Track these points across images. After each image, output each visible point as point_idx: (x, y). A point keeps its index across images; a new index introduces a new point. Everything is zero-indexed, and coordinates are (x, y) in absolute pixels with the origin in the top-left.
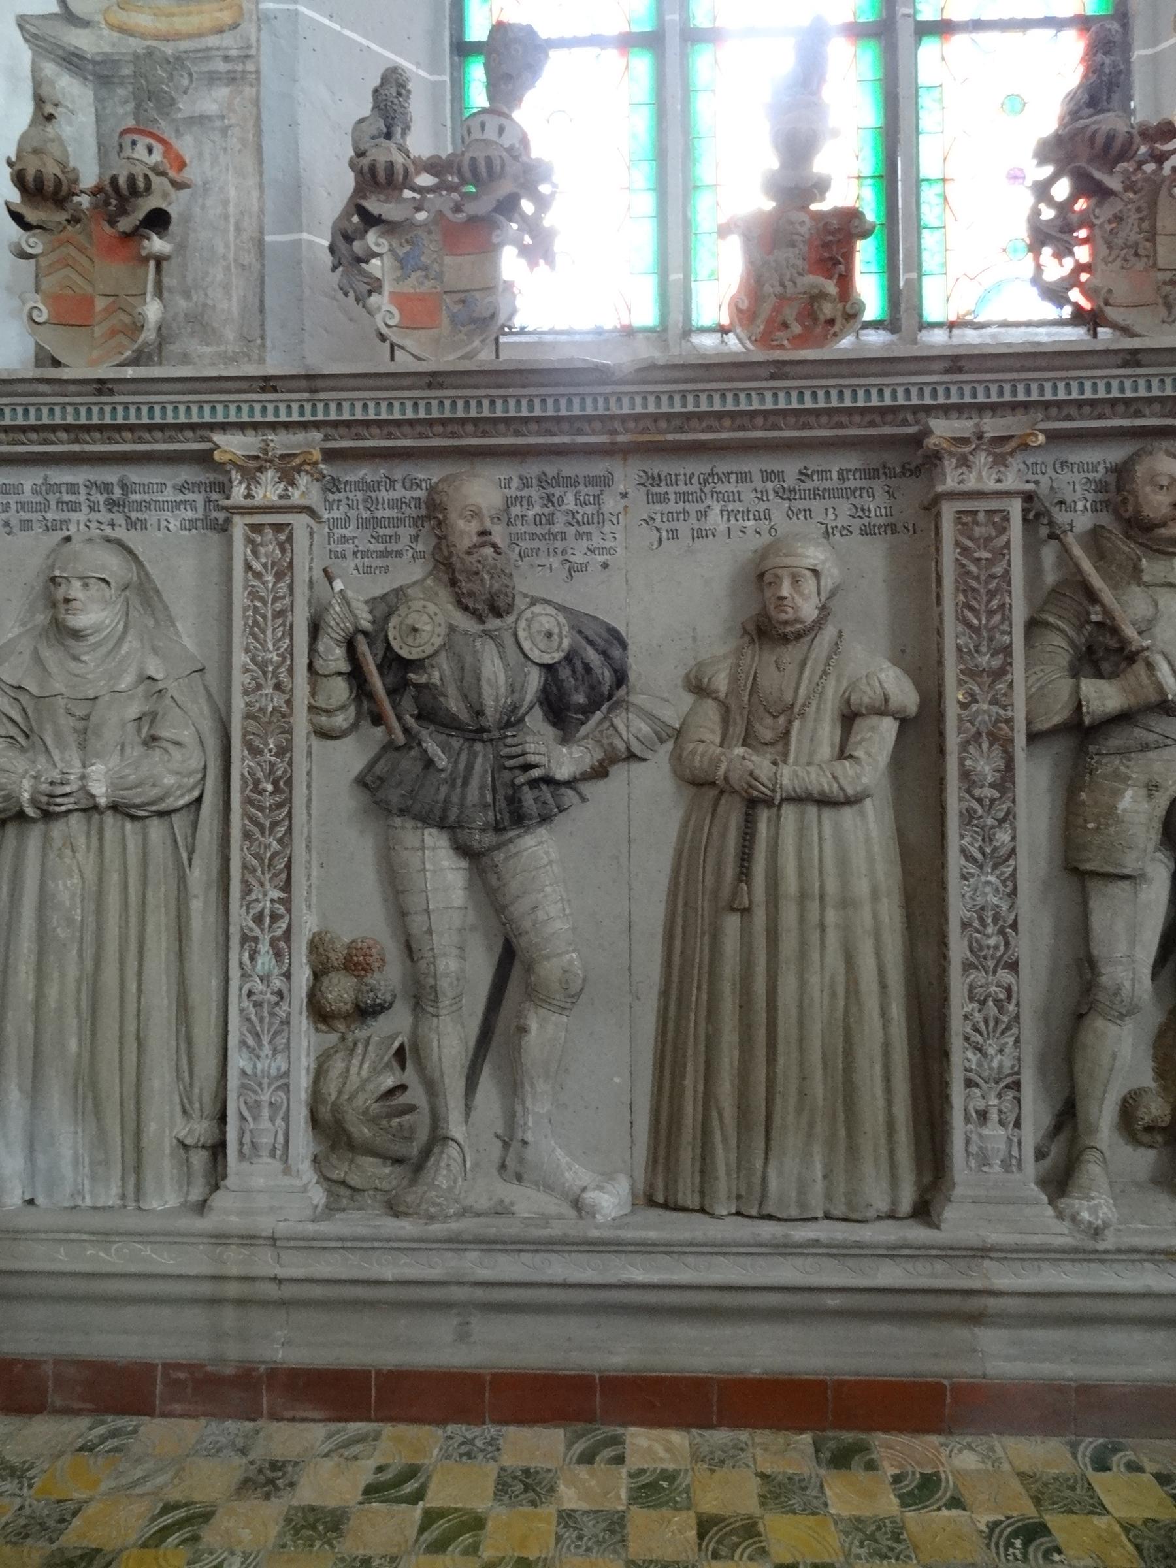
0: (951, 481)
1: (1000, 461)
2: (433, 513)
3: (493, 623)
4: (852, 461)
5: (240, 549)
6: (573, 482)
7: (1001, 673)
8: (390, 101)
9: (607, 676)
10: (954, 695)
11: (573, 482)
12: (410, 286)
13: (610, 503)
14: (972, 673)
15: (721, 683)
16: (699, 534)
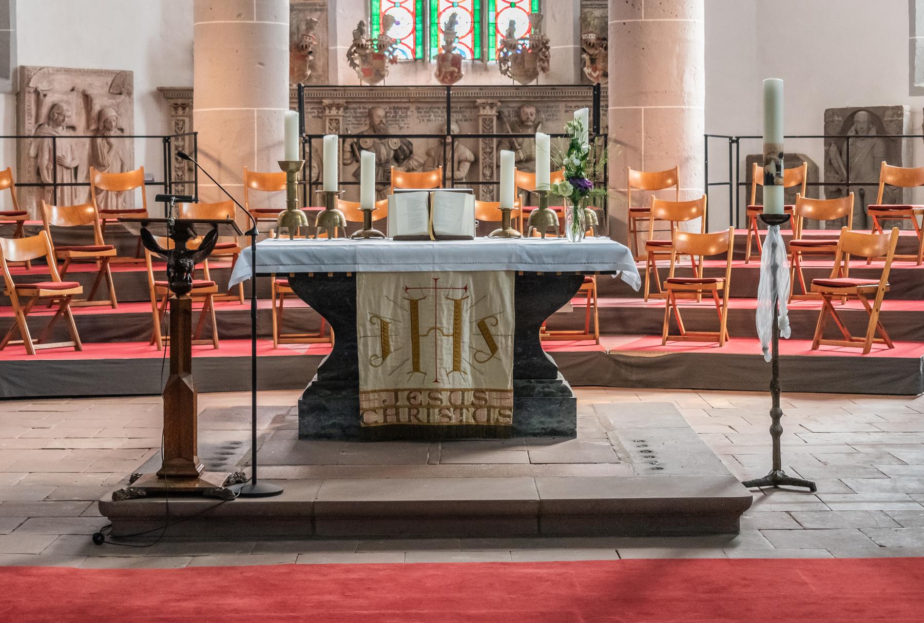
0: (482, 112)
1: (492, 108)
2: (370, 115)
3: (383, 141)
4: (462, 105)
5: (328, 124)
6: (400, 108)
7: (491, 153)
8: (360, 30)
9: (408, 152)
10: (481, 157)
11: (400, 108)
12: (365, 67)
13: (409, 113)
14: (485, 153)
15: (433, 154)
16: (429, 120)
